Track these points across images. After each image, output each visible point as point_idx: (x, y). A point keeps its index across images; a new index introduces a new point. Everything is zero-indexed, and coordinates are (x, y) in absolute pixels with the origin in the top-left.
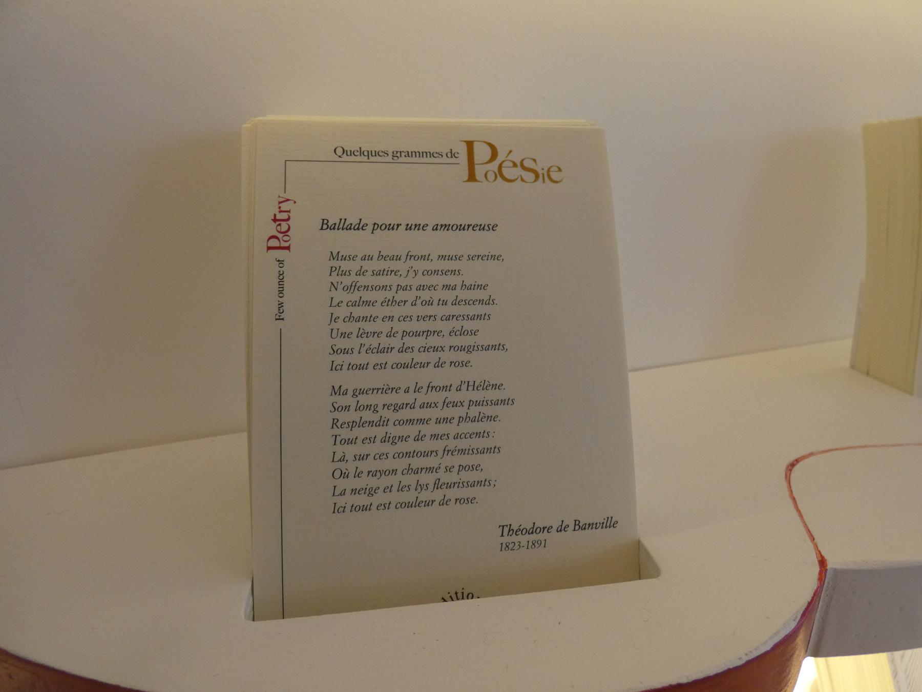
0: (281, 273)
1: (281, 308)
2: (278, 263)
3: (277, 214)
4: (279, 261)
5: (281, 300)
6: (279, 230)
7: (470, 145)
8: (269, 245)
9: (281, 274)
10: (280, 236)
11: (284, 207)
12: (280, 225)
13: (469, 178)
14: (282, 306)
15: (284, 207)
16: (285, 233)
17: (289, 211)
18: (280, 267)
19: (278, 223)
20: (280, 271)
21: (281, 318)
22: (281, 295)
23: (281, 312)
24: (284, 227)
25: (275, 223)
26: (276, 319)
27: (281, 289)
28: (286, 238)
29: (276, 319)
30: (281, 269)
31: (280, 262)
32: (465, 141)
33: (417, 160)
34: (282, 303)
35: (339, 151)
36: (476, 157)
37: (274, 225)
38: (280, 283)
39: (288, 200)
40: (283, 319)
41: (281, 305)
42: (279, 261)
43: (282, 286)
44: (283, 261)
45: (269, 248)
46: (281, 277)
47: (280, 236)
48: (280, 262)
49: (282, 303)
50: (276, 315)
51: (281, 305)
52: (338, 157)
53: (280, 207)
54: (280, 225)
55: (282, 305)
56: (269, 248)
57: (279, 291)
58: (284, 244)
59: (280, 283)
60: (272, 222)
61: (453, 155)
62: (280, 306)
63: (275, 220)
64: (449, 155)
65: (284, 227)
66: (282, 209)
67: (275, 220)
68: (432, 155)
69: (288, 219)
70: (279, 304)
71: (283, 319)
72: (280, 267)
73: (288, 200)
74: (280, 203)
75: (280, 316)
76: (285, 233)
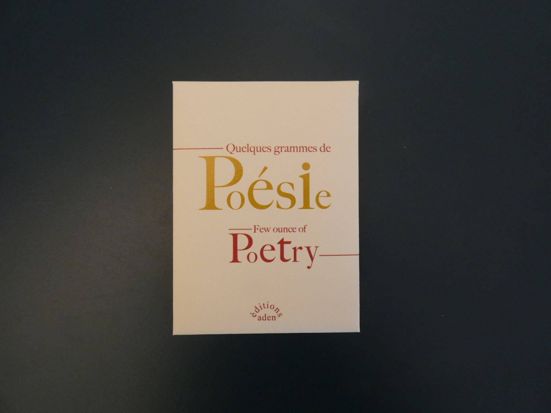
0: (294, 230)
1: (264, 230)
2: (303, 227)
4: (305, 228)
5: (272, 229)
14: (266, 232)
18: (299, 229)
20: (296, 229)
21: (256, 230)
22: (275, 230)
23: (261, 230)
26: (255, 226)
27: (280, 230)
29: (255, 226)
30: (298, 230)
34: (268, 232)
41: (267, 230)
42: (305, 228)
43: (283, 231)
44: (305, 232)
49: (268, 232)
50: (259, 226)
51: (267, 230)
55: (267, 231)
57: (279, 228)
59: (286, 229)
62: (266, 229)
70: (267, 228)
72: (299, 229)
75: (258, 229)
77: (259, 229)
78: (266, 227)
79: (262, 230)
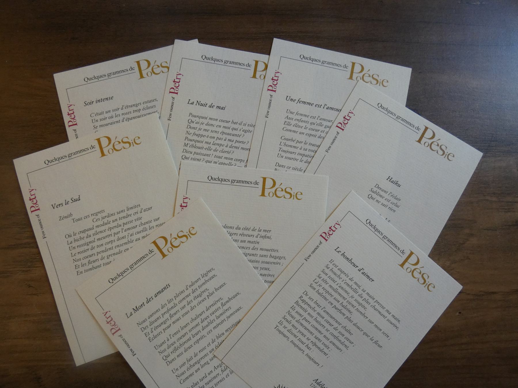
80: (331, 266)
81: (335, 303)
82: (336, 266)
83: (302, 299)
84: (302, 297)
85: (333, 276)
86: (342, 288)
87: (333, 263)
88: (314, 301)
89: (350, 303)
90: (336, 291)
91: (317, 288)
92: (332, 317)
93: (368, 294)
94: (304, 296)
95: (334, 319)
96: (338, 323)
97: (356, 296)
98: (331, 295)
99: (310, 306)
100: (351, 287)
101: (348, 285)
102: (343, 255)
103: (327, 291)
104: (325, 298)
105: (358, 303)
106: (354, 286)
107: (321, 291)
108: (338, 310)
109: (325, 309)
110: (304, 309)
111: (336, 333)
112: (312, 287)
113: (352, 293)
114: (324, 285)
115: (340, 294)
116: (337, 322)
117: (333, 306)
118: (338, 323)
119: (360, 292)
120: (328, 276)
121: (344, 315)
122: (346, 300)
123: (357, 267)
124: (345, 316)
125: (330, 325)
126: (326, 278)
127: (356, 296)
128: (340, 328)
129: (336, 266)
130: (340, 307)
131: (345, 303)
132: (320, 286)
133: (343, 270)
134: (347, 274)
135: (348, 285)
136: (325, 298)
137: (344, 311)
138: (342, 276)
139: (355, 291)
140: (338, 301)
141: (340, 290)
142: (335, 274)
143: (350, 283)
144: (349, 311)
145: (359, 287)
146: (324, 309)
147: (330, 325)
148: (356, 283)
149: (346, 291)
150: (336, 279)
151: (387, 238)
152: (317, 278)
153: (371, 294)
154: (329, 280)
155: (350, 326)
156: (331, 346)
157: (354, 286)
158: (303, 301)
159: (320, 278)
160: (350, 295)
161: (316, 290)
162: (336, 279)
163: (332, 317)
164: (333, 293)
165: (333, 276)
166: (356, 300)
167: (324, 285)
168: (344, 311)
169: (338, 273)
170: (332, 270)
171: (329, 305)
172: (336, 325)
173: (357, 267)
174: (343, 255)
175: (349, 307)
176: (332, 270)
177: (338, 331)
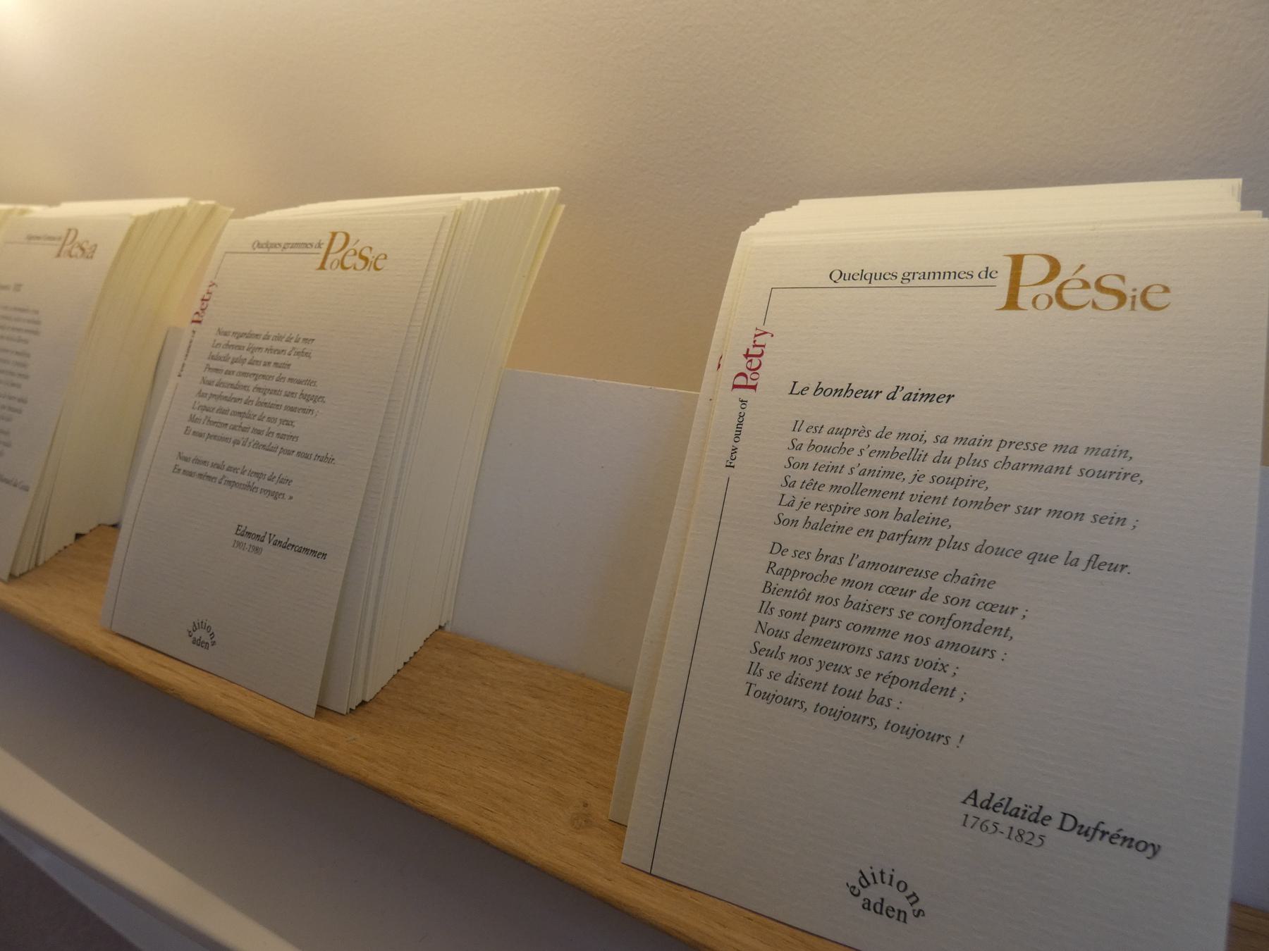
3: (751, 348)
4: (742, 401)
6: (749, 367)
7: (1017, 261)
8: (735, 384)
9: (741, 416)
10: (749, 373)
11: (760, 341)
12: (751, 361)
13: (1007, 303)
15: (760, 341)
16: (754, 370)
17: (764, 346)
19: (749, 358)
21: (732, 465)
22: (737, 439)
24: (755, 363)
25: (747, 358)
26: (727, 466)
28: (754, 376)
29: (727, 466)
31: (743, 402)
32: (1010, 256)
33: (936, 282)
34: (736, 449)
35: (836, 276)
36: (1023, 272)
37: (745, 361)
38: (739, 426)
39: (765, 333)
40: (733, 467)
41: (734, 450)
42: (742, 401)
43: (738, 429)
45: (735, 386)
46: (741, 420)
47: (749, 373)
48: (743, 402)
51: (734, 450)
52: (833, 282)
53: (755, 341)
54: (751, 361)
56: (735, 386)
58: (751, 383)
59: (739, 426)
60: (743, 357)
61: (988, 273)
63: (747, 355)
64: (983, 275)
65: (755, 363)
66: (757, 343)
67: (747, 355)
68: (957, 275)
69: (761, 355)
71: (733, 467)
73: (765, 333)
74: (756, 336)
76: (754, 370)
77: (731, 461)
78: (730, 451)
79: (734, 457)
80: (804, 438)
81: (877, 524)
82: (818, 429)
83: (775, 569)
84: (772, 565)
85: (825, 458)
86: (872, 472)
87: (804, 427)
88: (813, 556)
89: (923, 499)
90: (858, 490)
91: (801, 516)
92: (893, 569)
93: (961, 440)
94: (777, 558)
95: (904, 571)
96: (924, 574)
97: (928, 468)
98: (852, 511)
99: (809, 577)
100: (895, 454)
101: (884, 454)
102: (820, 390)
103: (833, 508)
104: (841, 529)
105: (948, 481)
106: (904, 446)
107: (817, 516)
108: (901, 539)
109: (861, 559)
110: (797, 594)
111: (939, 608)
112: (786, 522)
113: (909, 468)
114: (813, 496)
115: (875, 492)
116: (918, 573)
117: (876, 535)
118: (924, 574)
119: (933, 449)
120: (811, 465)
121: (928, 541)
122: (906, 498)
123: (878, 393)
124: (934, 543)
125: (904, 593)
126: (808, 474)
127: (928, 468)
128: (940, 587)
129: (818, 429)
130: (900, 527)
131: (908, 508)
132: (804, 505)
133: (843, 426)
134: (861, 429)
135: (884, 454)
136: (841, 529)
137: (919, 530)
138: (851, 441)
139: (917, 457)
140: (885, 514)
141: (870, 482)
142: (827, 450)
143: (886, 444)
144: (936, 521)
145: (920, 438)
146: (855, 562)
147: (904, 593)
148: (904, 436)
149: (890, 474)
150: (838, 460)
151: (916, 275)
152: (787, 491)
153: (970, 434)
154: (820, 477)
155: (968, 563)
156: (946, 655)
157: (904, 446)
158: (784, 572)
159: (792, 485)
160: (909, 476)
161: (801, 524)
162: (838, 460)
163: (893, 569)
164: (853, 500)
165: (825, 458)
166: (934, 479)
167: (813, 496)
168: (919, 530)
169: (835, 441)
170: (812, 446)
171: (865, 540)
172: (921, 585)
173: (878, 393)
174: (820, 390)
175: (926, 510)
176: (812, 446)
177: (942, 598)
